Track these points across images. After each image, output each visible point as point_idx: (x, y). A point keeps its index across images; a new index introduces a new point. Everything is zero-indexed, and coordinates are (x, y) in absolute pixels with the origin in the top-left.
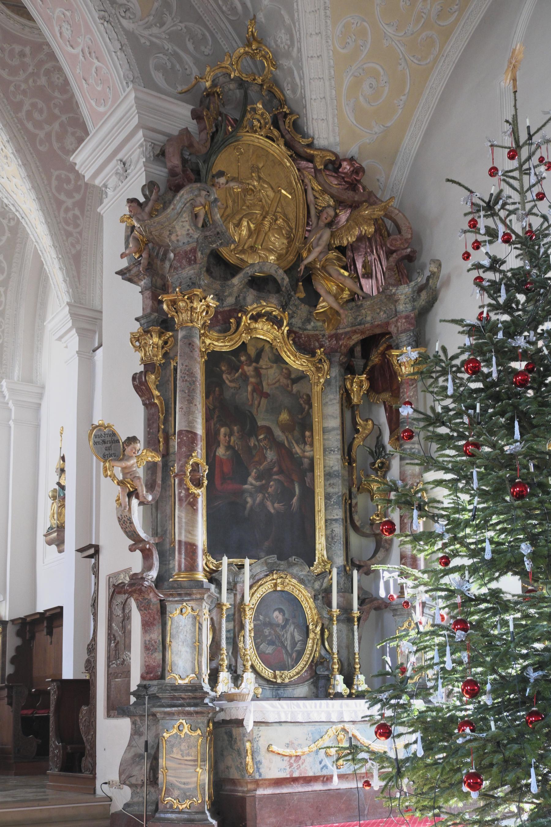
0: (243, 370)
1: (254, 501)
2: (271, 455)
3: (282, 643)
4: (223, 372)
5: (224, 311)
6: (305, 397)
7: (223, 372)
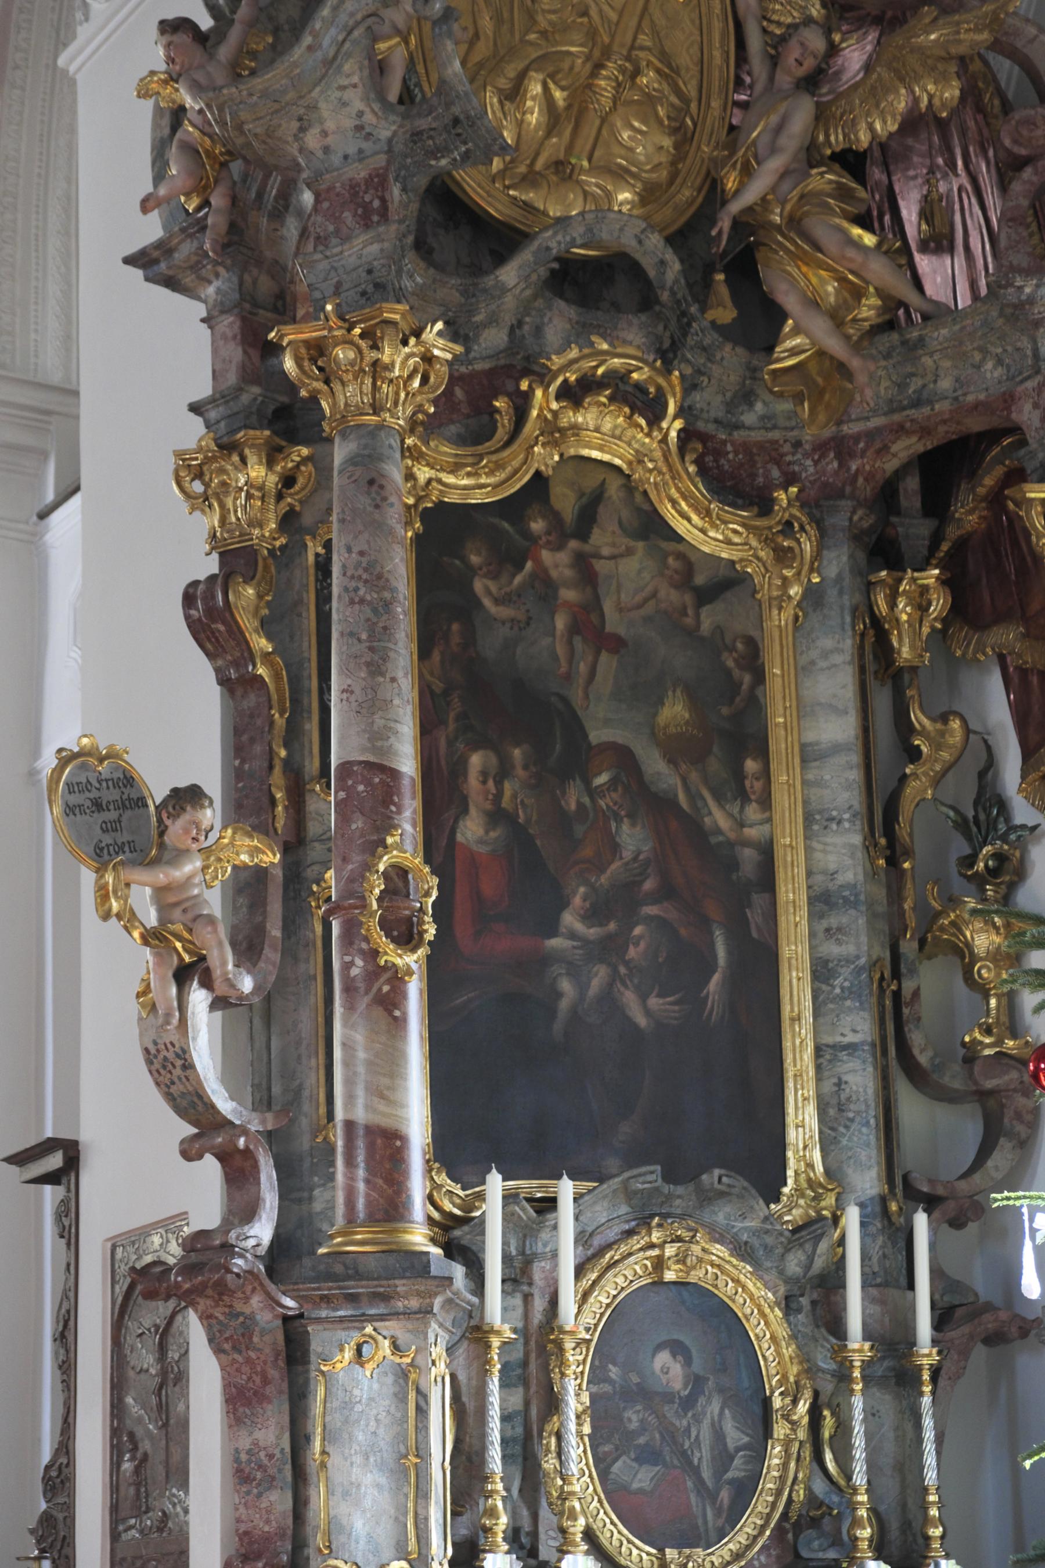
0: (538, 561)
1: (582, 988)
2: (633, 839)
3: (685, 1457)
4: (472, 571)
5: (473, 375)
6: (740, 646)
7: (472, 571)
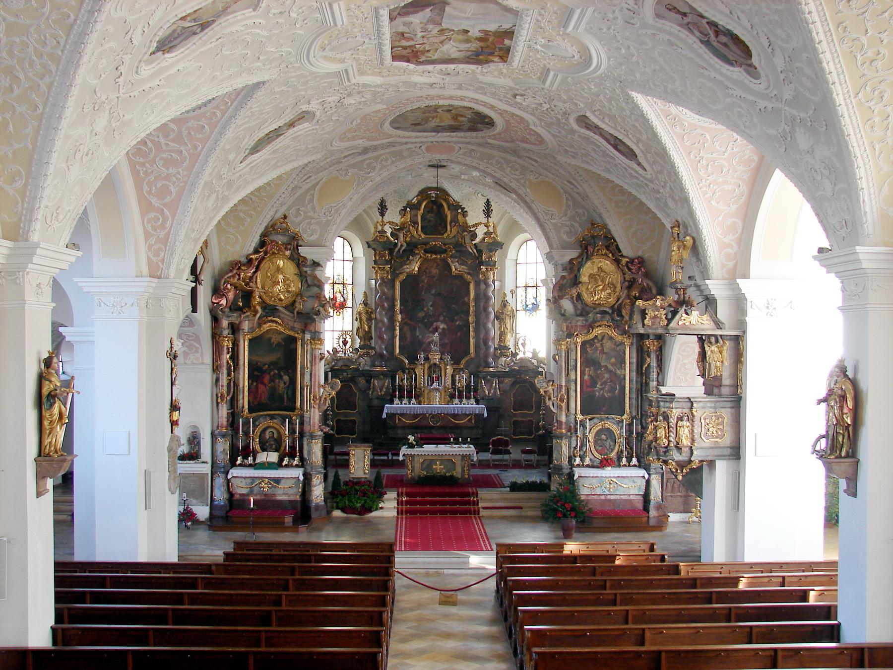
2: (607, 376)
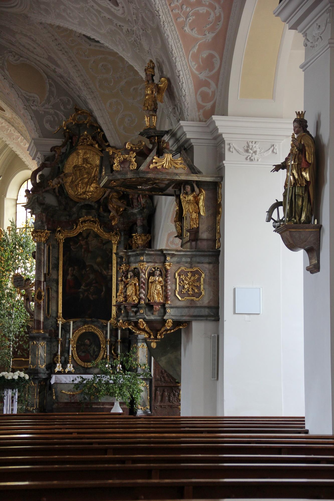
2: (92, 276)
